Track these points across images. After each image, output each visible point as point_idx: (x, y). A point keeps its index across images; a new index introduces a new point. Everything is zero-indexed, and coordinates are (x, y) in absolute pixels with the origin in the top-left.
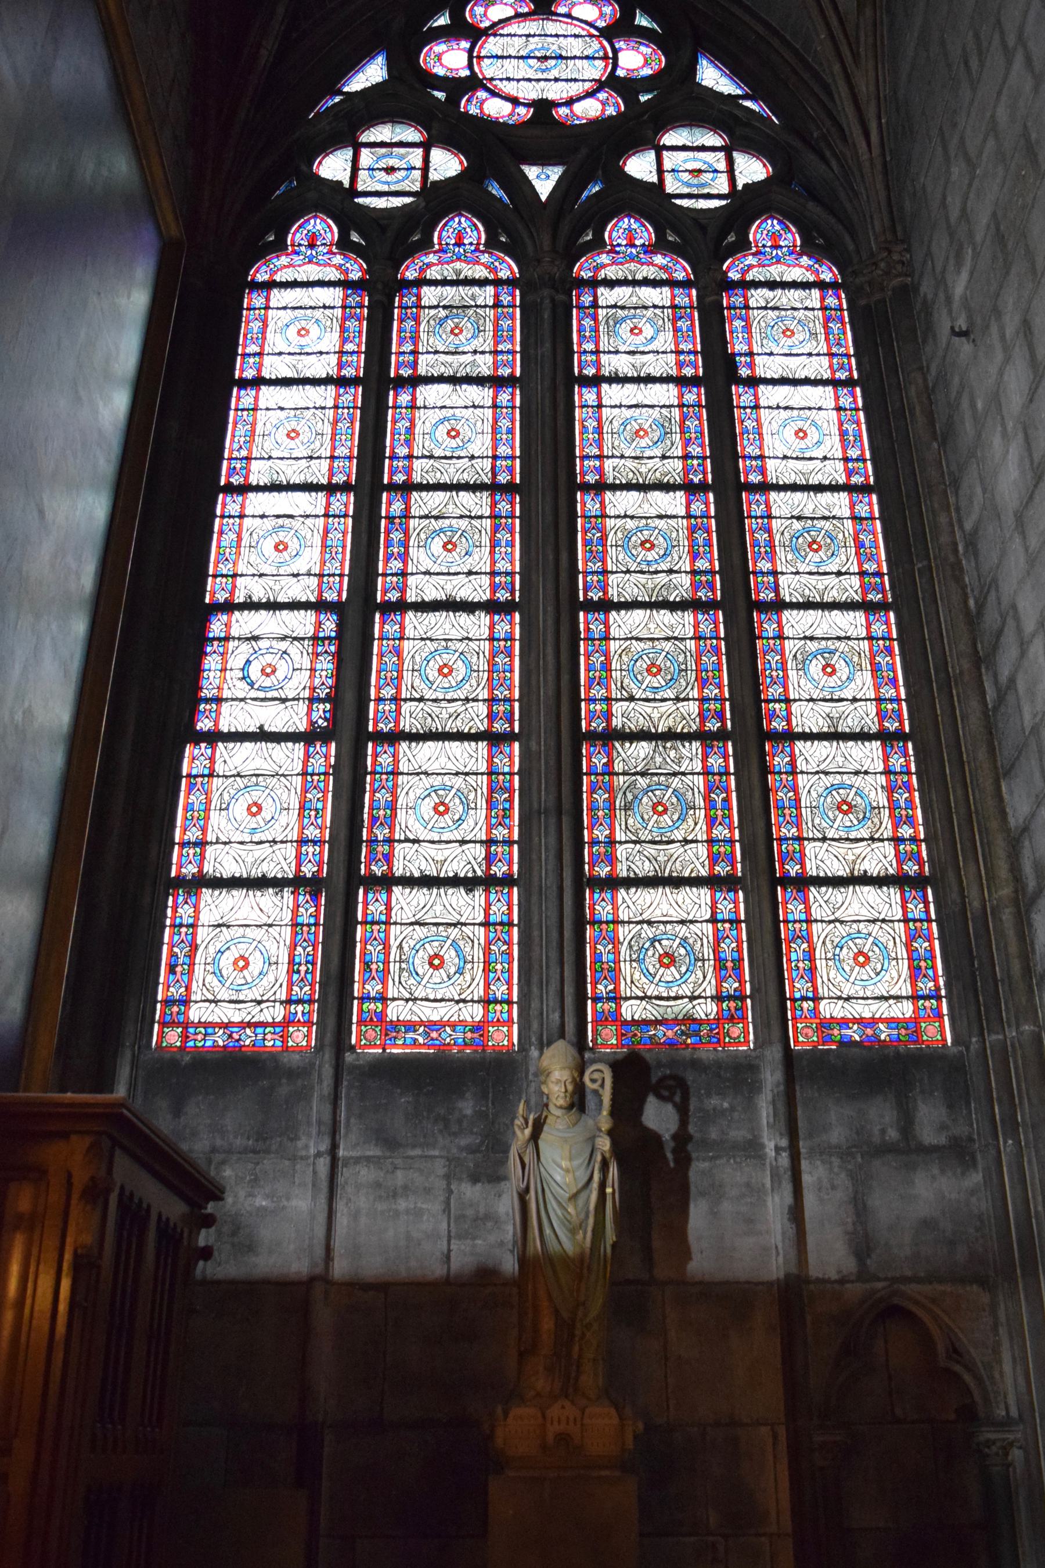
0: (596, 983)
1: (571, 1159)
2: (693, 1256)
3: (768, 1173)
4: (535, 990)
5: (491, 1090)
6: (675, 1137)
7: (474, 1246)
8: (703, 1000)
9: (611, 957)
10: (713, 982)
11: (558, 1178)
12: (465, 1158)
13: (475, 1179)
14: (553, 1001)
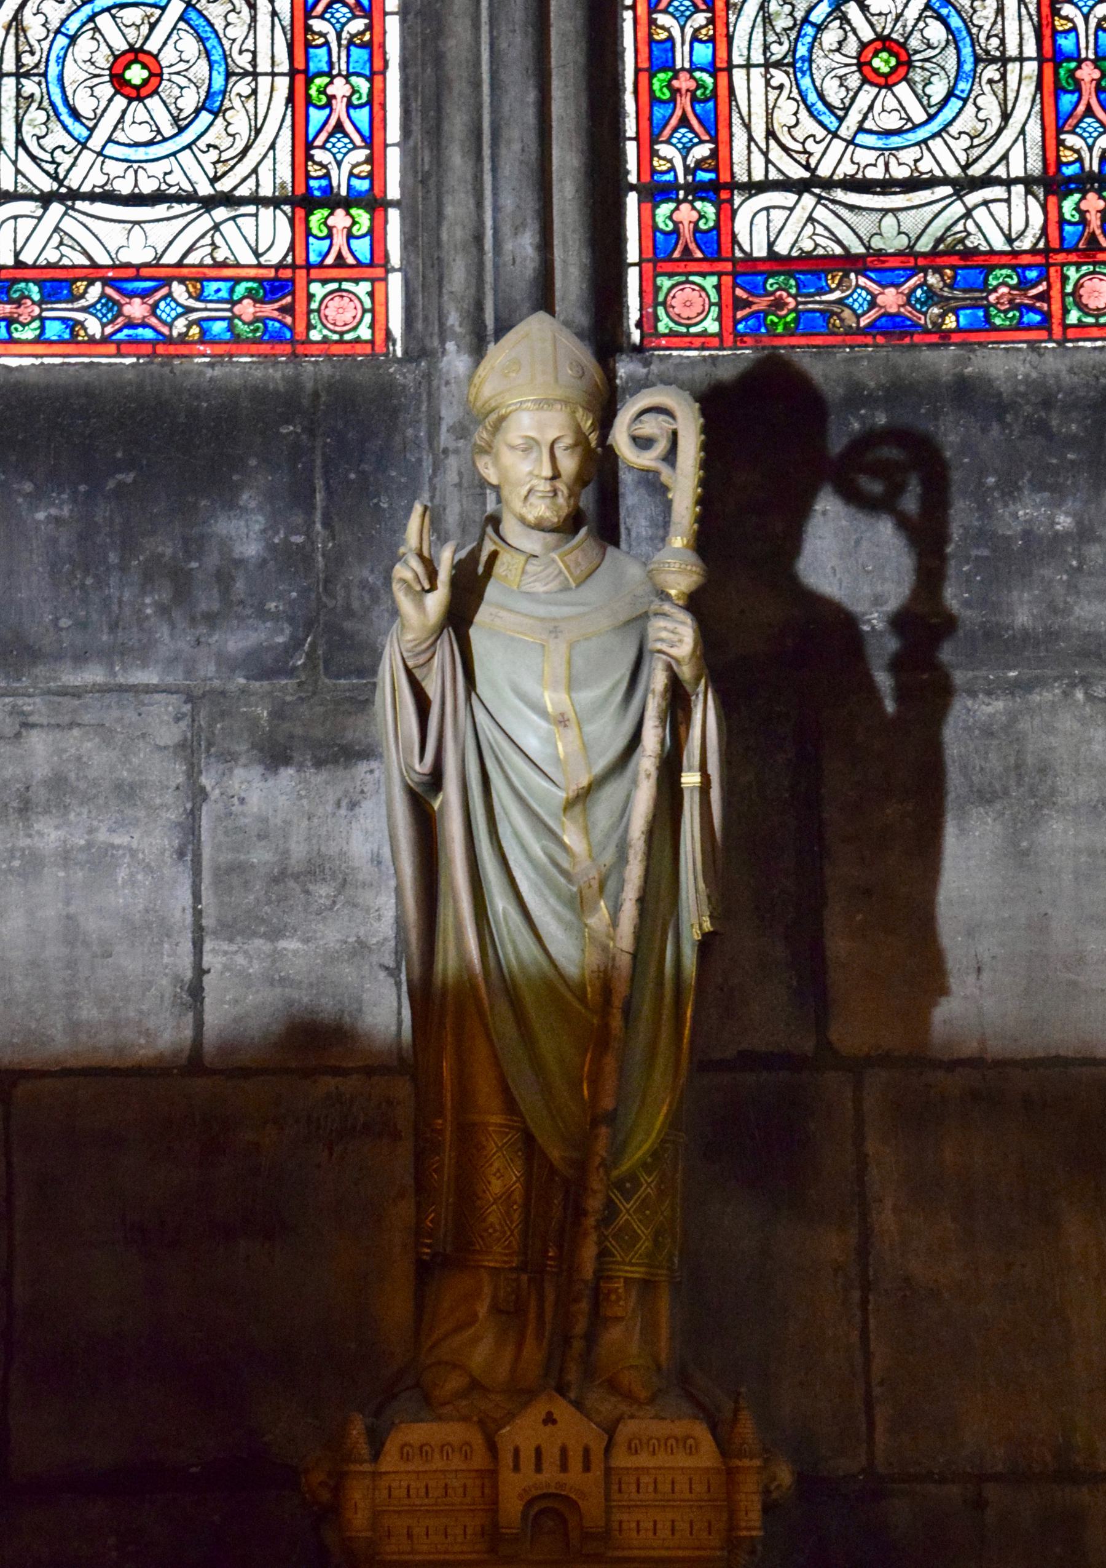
0: (654, 140)
1: (572, 684)
2: (953, 982)
4: (457, 160)
5: (319, 483)
6: (900, 622)
7: (276, 956)
8: (999, 192)
9: (703, 53)
10: (1034, 130)
11: (532, 744)
12: (243, 691)
13: (275, 755)
14: (513, 196)
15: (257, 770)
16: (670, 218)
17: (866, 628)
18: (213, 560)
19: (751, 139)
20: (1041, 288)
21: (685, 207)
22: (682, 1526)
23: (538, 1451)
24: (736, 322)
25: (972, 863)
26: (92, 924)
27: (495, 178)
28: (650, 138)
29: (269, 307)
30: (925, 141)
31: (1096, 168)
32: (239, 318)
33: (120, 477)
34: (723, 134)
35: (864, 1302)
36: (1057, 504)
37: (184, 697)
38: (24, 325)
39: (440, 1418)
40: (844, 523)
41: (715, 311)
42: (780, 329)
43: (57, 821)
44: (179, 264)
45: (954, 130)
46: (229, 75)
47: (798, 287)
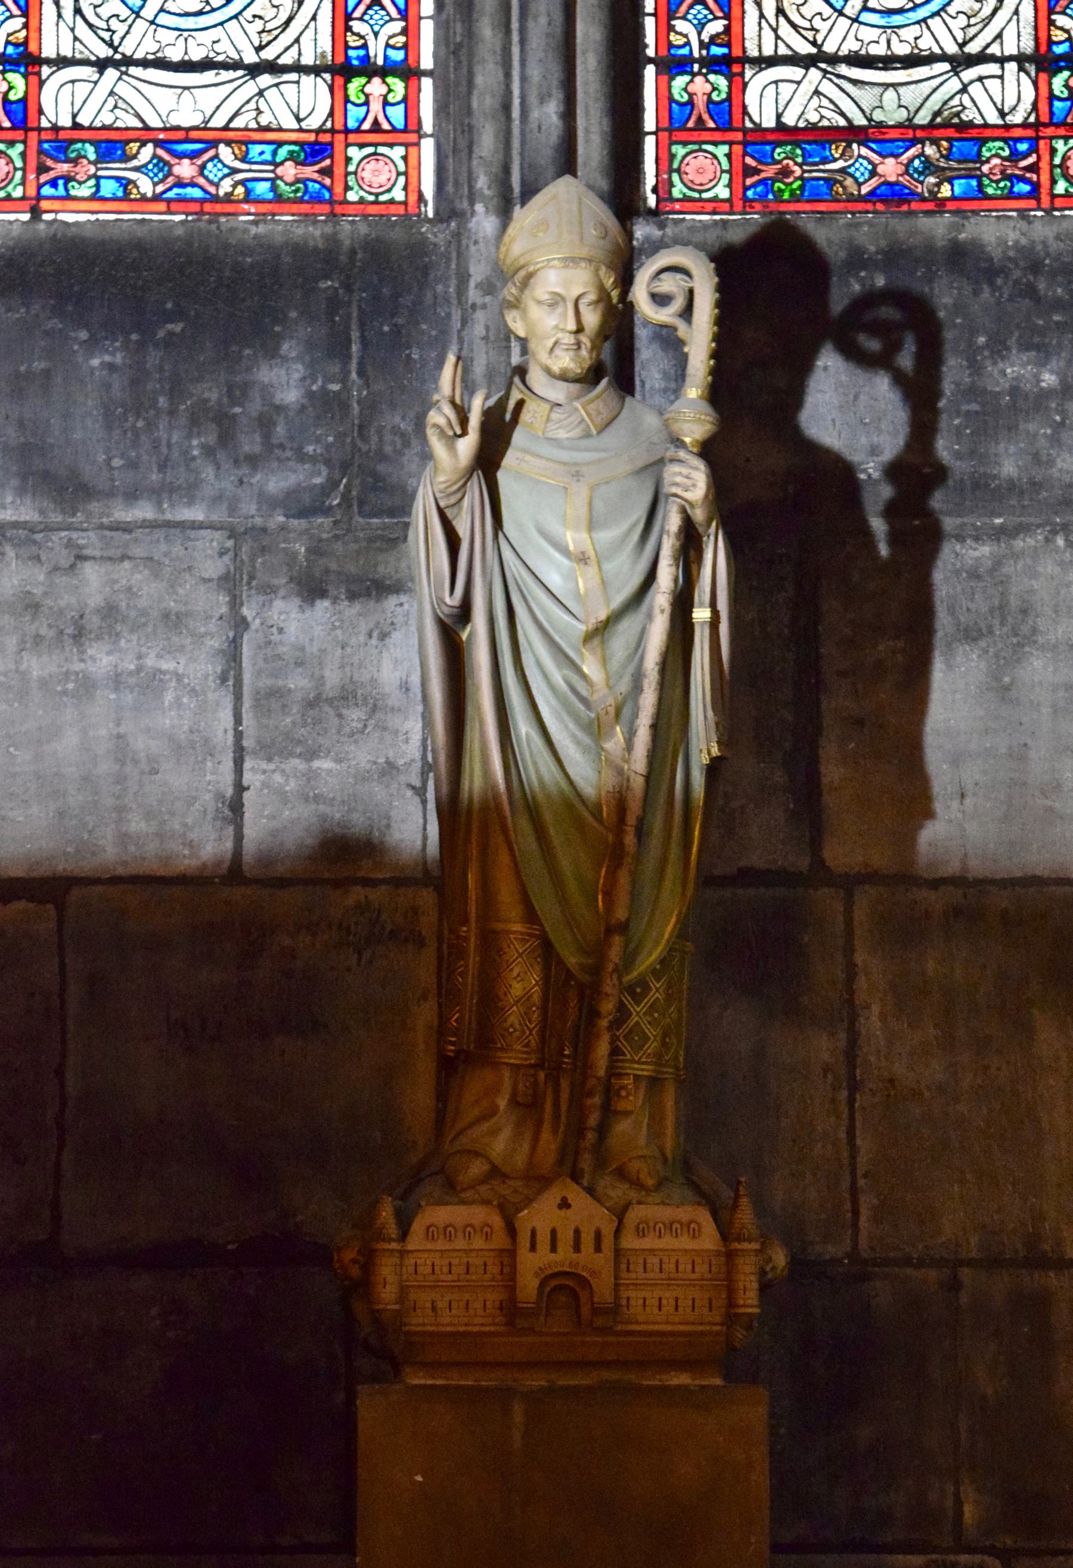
0: (671, 15)
1: (592, 525)
2: (938, 806)
4: (487, 30)
5: (355, 334)
6: (894, 471)
7: (311, 776)
8: (993, 68)
11: (554, 580)
12: (283, 528)
13: (311, 589)
14: (539, 67)
15: (297, 601)
16: (685, 90)
17: (863, 476)
18: (255, 406)
19: (762, 16)
20: (1031, 160)
21: (699, 79)
22: (685, 1303)
23: (554, 1232)
24: (746, 189)
25: (958, 696)
26: (140, 744)
27: (522, 50)
30: (924, 20)
32: (281, 178)
33: (170, 326)
34: (736, 12)
35: (851, 1101)
36: (1042, 364)
37: (226, 533)
38: (80, 183)
39: (463, 1202)
40: (843, 378)
41: (726, 178)
42: (786, 196)
43: (108, 647)
44: (226, 128)
47: (803, 156)
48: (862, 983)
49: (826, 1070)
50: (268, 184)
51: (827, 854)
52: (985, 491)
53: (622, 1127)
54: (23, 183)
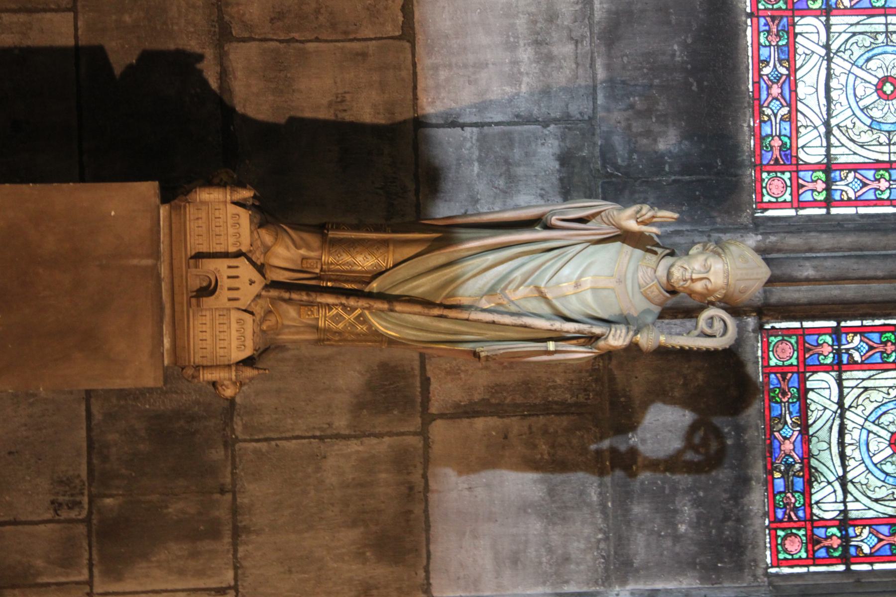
1: (594, 289)
2: (464, 478)
3: (585, 589)
4: (849, 240)
5: (694, 178)
6: (633, 452)
7: (470, 162)
8: (840, 497)
10: (870, 514)
11: (566, 271)
12: (595, 144)
13: (564, 159)
14: (831, 267)
15: (558, 151)
17: (630, 435)
18: (656, 128)
19: (864, 380)
20: (794, 518)
21: (830, 349)
23: (237, 277)
25: (520, 486)
26: (483, 75)
27: (840, 257)
28: (861, 331)
29: (778, 153)
30: (864, 462)
31: (852, 543)
33: (695, 84)
34: (865, 367)
35: (314, 437)
36: (690, 524)
37: (591, 116)
38: (767, 38)
39: (252, 232)
40: (680, 424)
41: (780, 363)
42: (772, 394)
43: (532, 58)
44: (797, 110)
45: (870, 476)
46: (889, 132)
48: (374, 441)
49: (330, 425)
50: (769, 132)
51: (439, 422)
52: (625, 497)
53: (292, 312)
54: (766, 9)
